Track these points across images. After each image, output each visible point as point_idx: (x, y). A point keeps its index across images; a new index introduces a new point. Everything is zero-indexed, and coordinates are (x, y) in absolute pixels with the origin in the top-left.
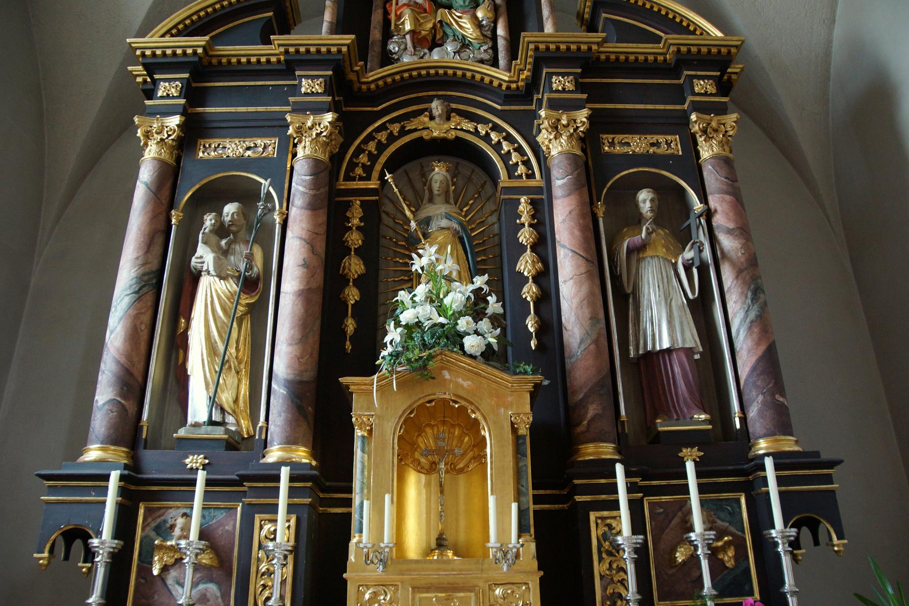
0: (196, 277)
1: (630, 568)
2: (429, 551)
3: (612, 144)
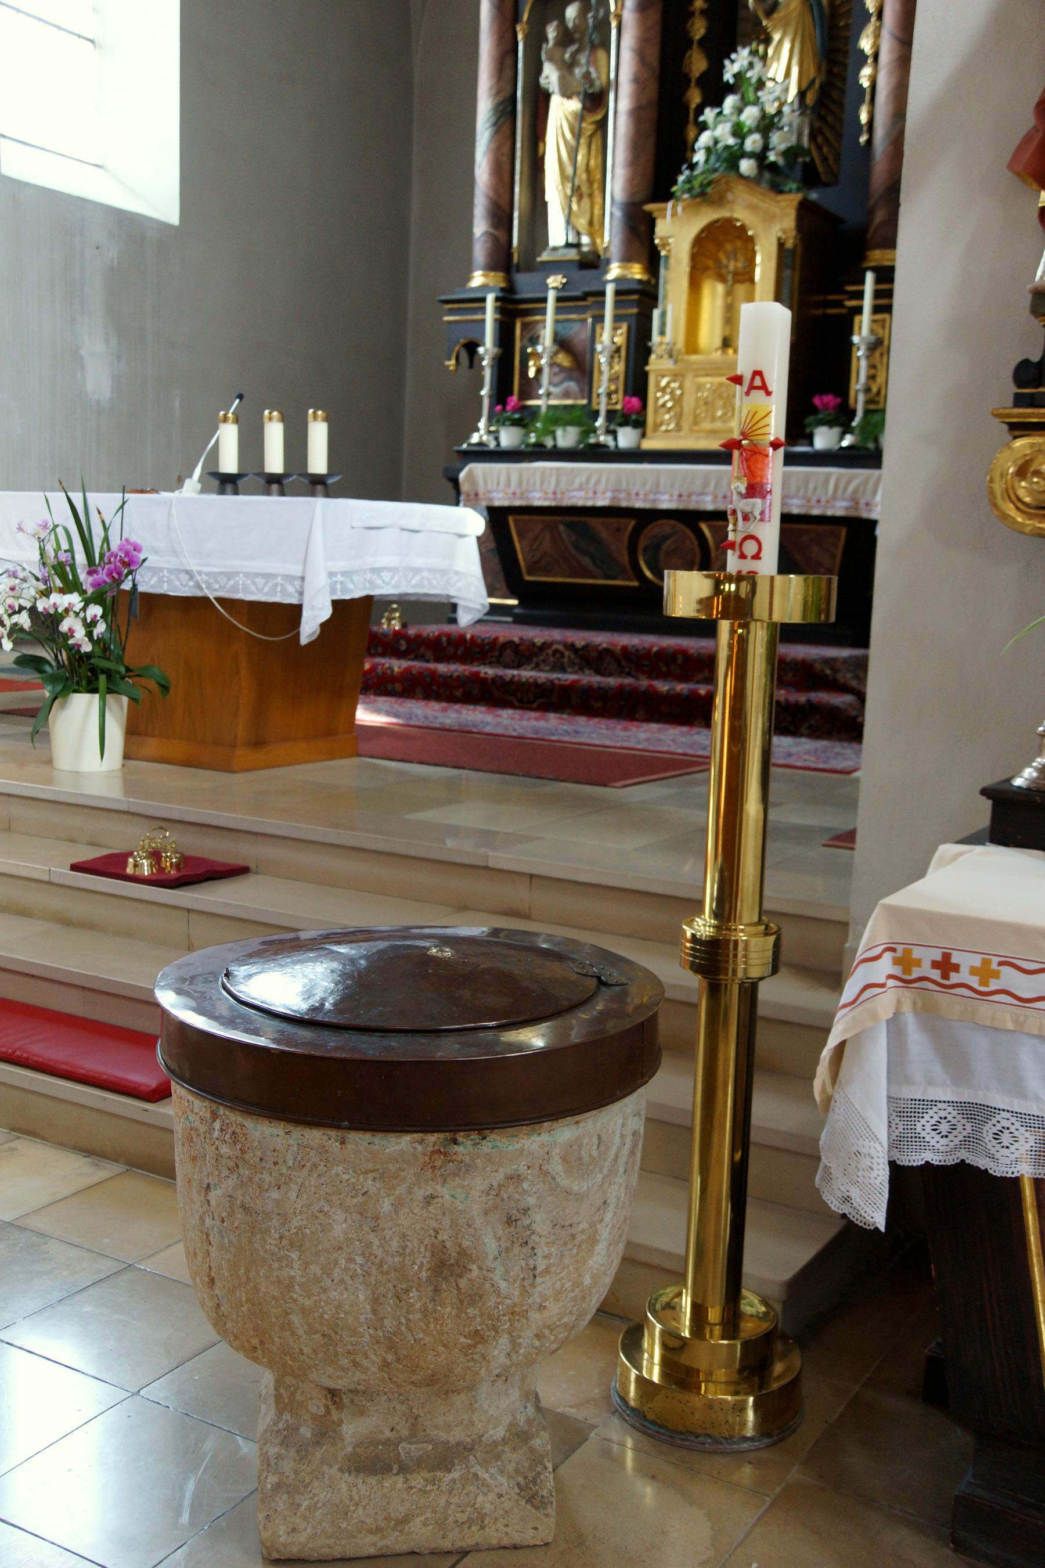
0: (547, 96)
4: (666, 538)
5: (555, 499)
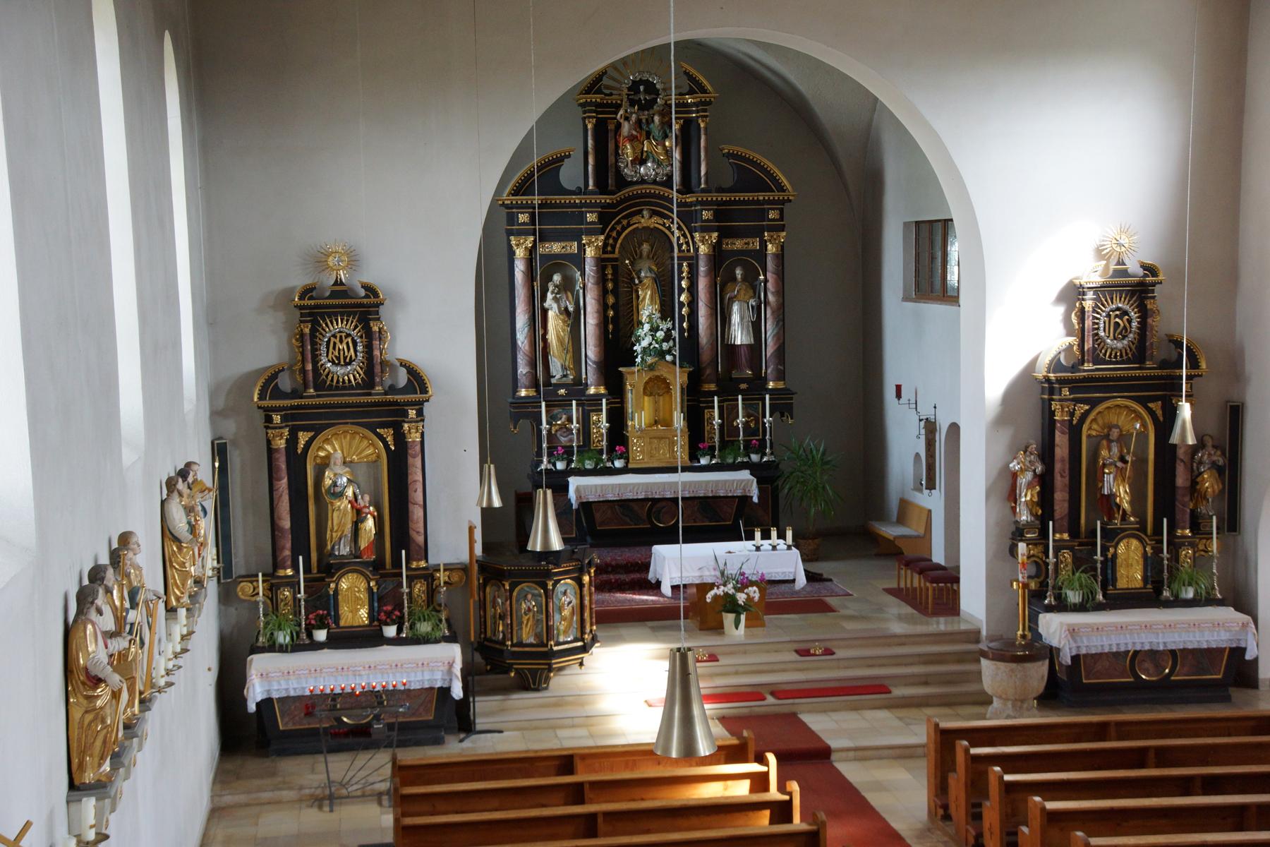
1: (717, 432)
2: (650, 426)
3: (727, 244)
4: (664, 507)
5: (619, 497)
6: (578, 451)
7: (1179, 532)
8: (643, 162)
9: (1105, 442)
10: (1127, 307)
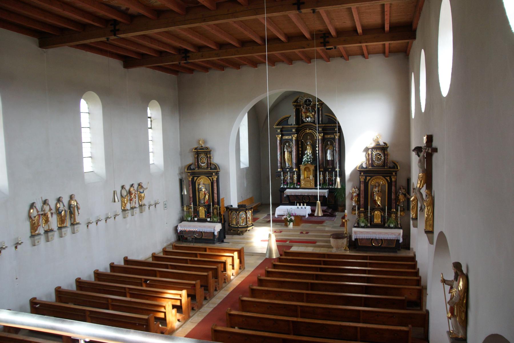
6: (290, 184)
7: (392, 210)
8: (308, 118)
9: (375, 187)
10: (381, 153)
